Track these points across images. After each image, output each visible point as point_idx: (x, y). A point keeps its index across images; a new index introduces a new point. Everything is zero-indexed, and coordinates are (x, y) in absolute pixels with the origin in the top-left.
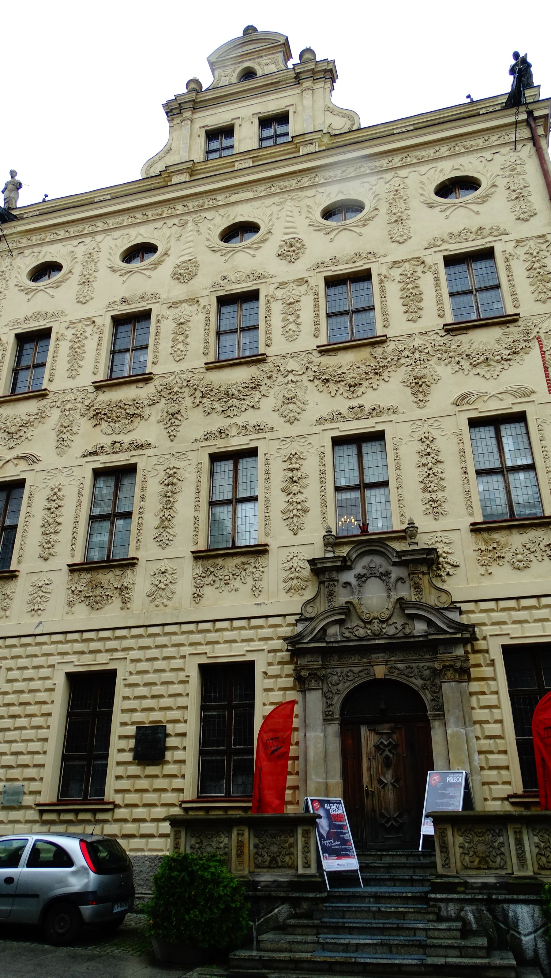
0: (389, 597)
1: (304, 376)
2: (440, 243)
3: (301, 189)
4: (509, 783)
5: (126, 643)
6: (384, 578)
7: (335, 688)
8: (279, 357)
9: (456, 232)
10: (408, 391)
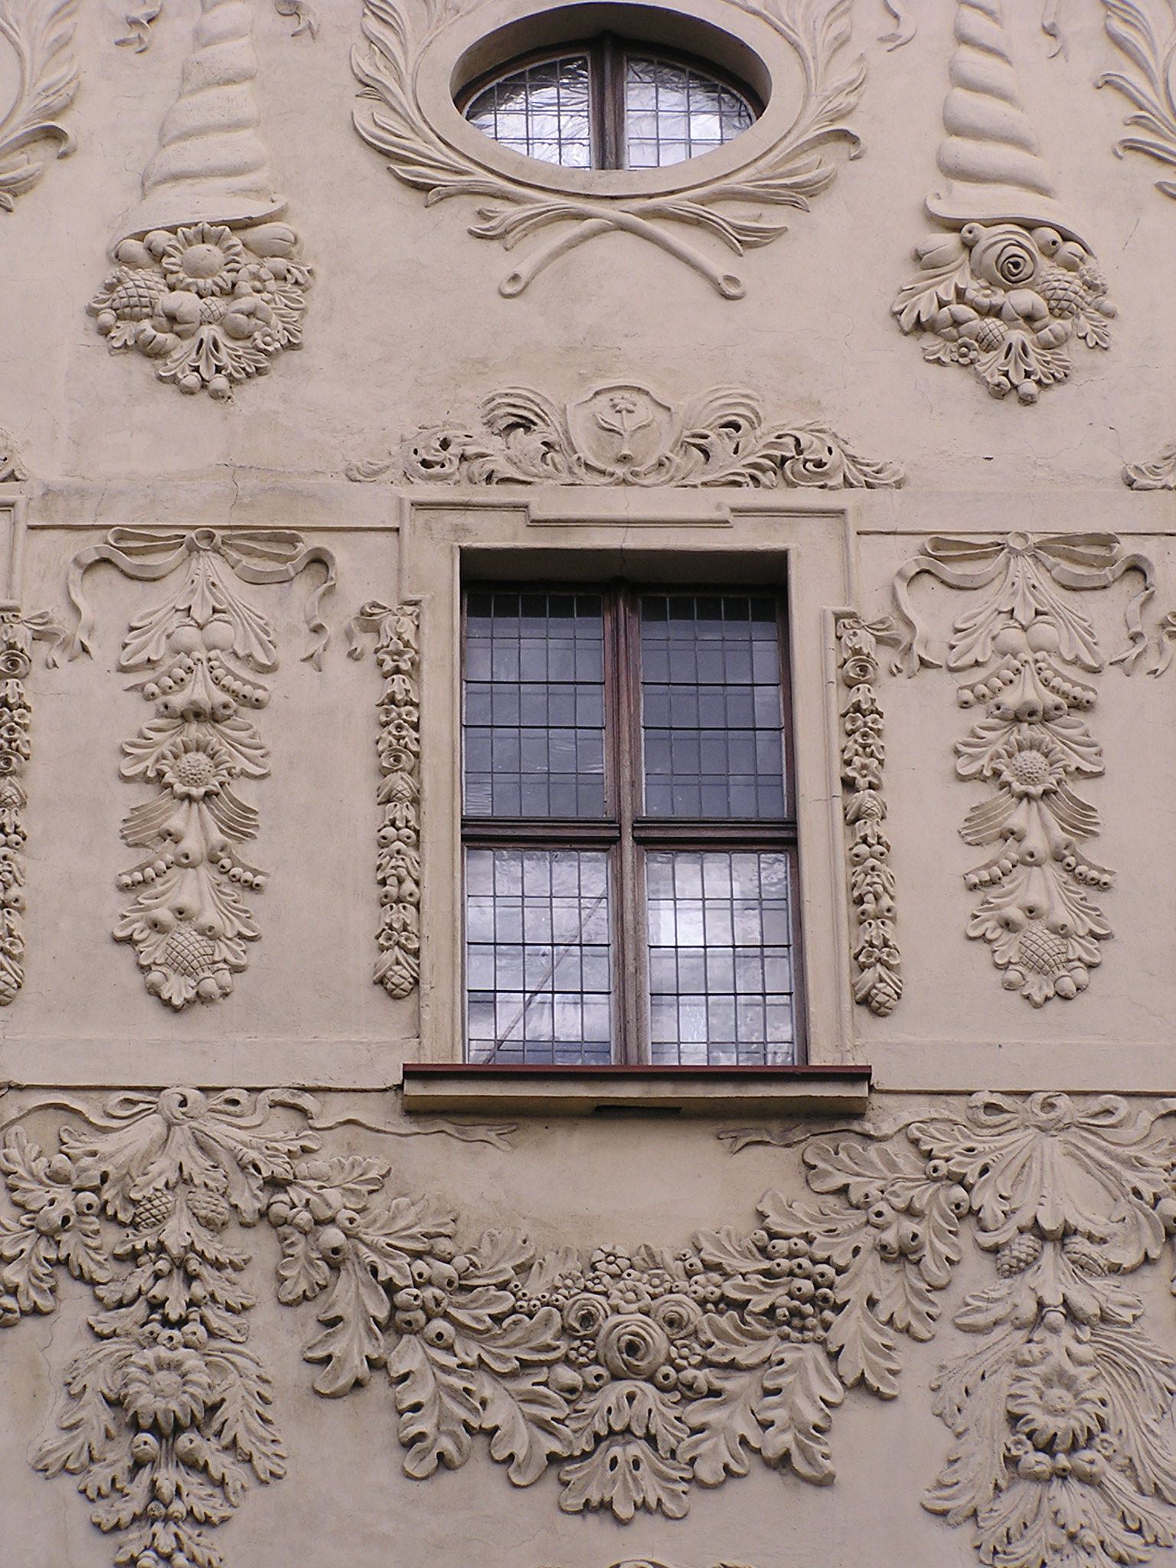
8: (955, 1108)
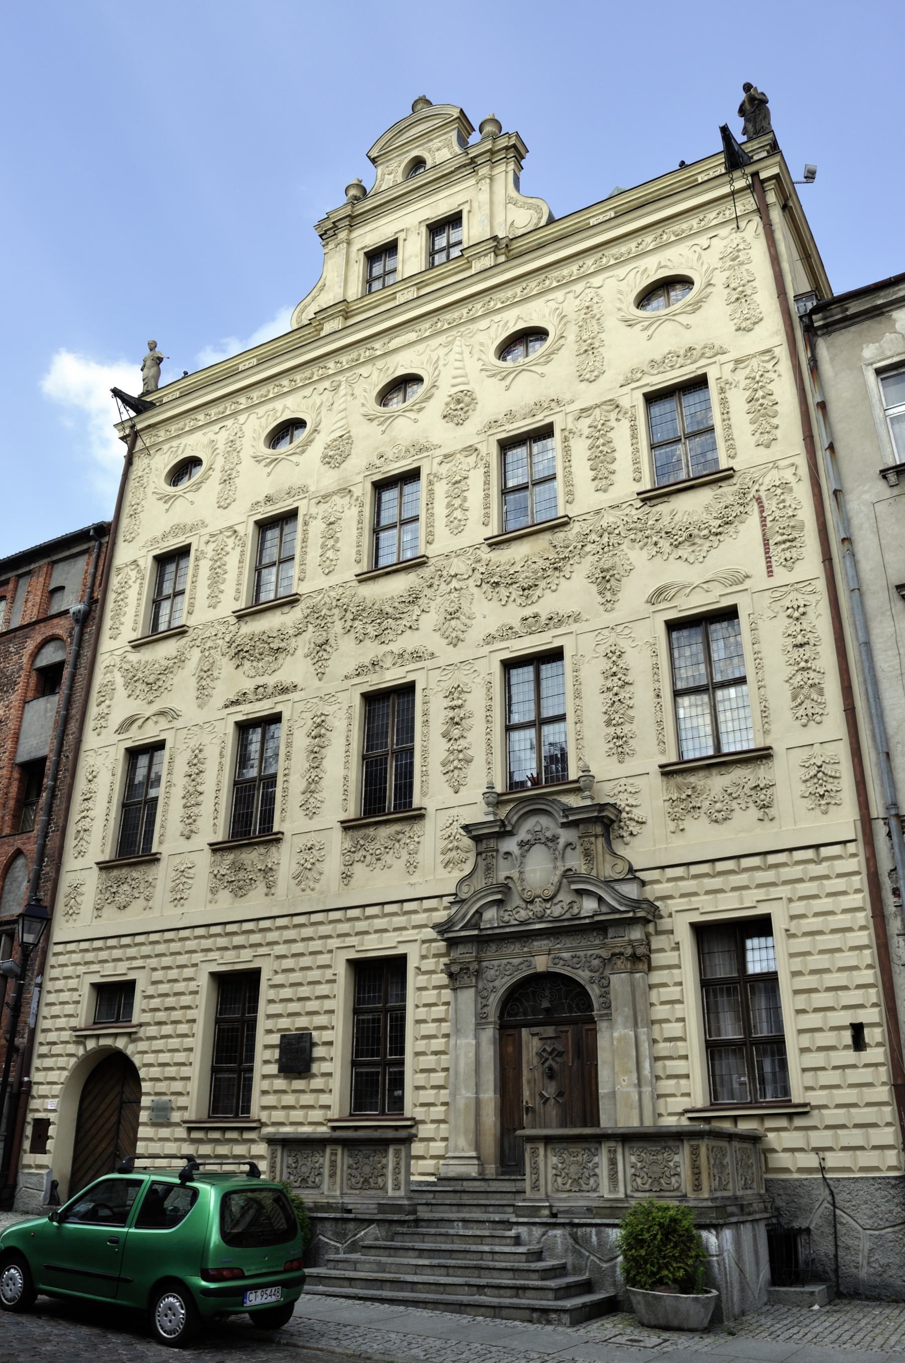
0: (555, 868)
1: (471, 580)
2: (639, 375)
3: (473, 320)
4: (689, 1095)
5: (272, 936)
6: (550, 844)
7: (491, 984)
9: (658, 358)
10: (594, 588)
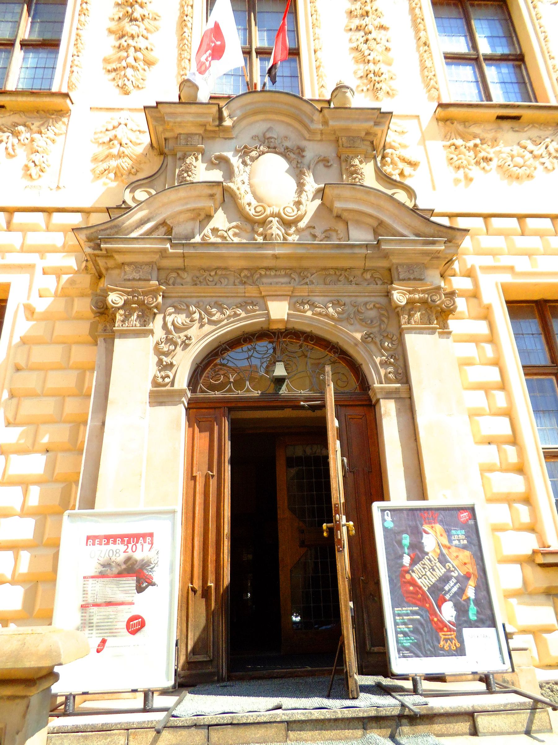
0: (301, 186)
